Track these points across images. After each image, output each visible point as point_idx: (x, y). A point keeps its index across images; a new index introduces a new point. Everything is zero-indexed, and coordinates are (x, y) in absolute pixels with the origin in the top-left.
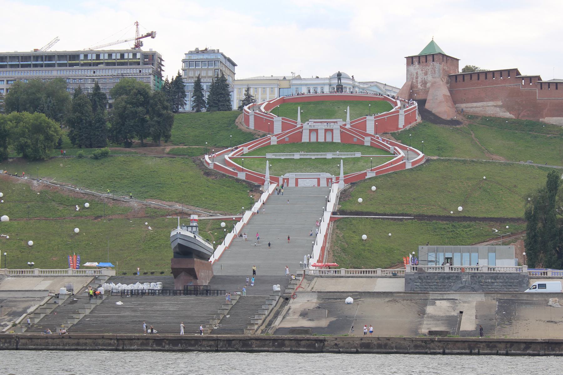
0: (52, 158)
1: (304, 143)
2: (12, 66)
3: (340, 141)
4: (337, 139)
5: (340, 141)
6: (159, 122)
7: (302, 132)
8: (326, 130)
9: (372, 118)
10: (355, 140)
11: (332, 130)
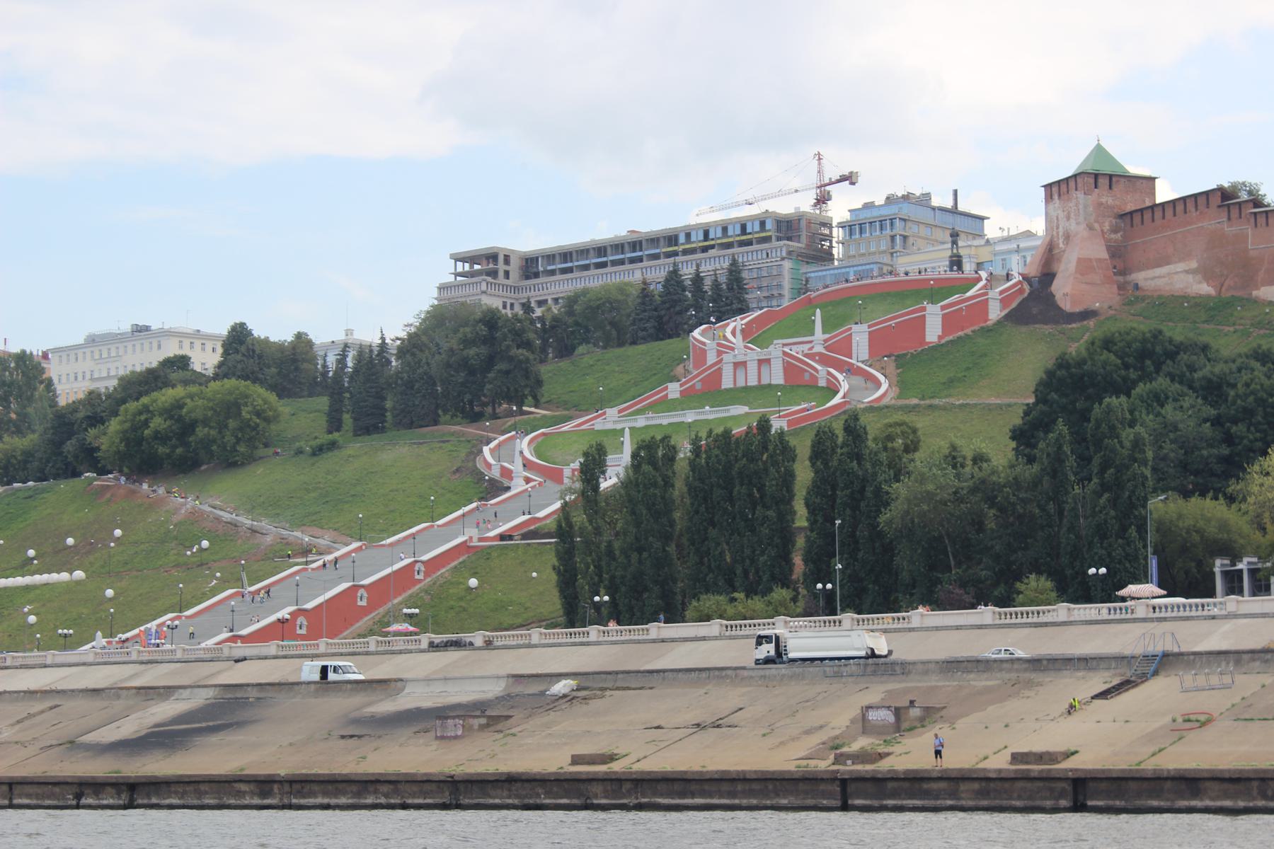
0: (261, 458)
1: (727, 390)
2: (614, 263)
3: (781, 382)
4: (778, 378)
5: (781, 382)
6: (508, 372)
7: (720, 369)
8: (761, 362)
9: (864, 328)
10: (807, 376)
11: (768, 361)
